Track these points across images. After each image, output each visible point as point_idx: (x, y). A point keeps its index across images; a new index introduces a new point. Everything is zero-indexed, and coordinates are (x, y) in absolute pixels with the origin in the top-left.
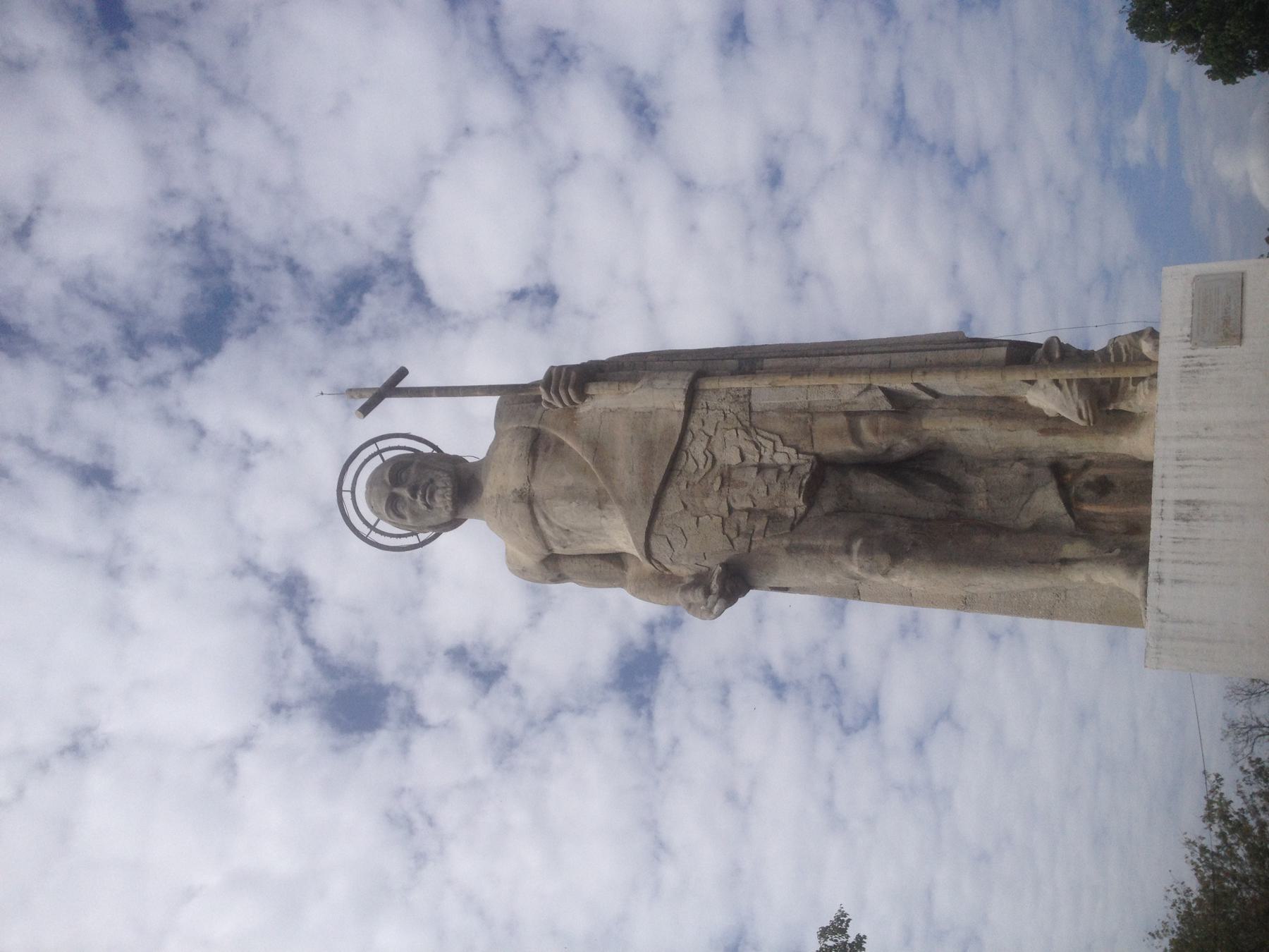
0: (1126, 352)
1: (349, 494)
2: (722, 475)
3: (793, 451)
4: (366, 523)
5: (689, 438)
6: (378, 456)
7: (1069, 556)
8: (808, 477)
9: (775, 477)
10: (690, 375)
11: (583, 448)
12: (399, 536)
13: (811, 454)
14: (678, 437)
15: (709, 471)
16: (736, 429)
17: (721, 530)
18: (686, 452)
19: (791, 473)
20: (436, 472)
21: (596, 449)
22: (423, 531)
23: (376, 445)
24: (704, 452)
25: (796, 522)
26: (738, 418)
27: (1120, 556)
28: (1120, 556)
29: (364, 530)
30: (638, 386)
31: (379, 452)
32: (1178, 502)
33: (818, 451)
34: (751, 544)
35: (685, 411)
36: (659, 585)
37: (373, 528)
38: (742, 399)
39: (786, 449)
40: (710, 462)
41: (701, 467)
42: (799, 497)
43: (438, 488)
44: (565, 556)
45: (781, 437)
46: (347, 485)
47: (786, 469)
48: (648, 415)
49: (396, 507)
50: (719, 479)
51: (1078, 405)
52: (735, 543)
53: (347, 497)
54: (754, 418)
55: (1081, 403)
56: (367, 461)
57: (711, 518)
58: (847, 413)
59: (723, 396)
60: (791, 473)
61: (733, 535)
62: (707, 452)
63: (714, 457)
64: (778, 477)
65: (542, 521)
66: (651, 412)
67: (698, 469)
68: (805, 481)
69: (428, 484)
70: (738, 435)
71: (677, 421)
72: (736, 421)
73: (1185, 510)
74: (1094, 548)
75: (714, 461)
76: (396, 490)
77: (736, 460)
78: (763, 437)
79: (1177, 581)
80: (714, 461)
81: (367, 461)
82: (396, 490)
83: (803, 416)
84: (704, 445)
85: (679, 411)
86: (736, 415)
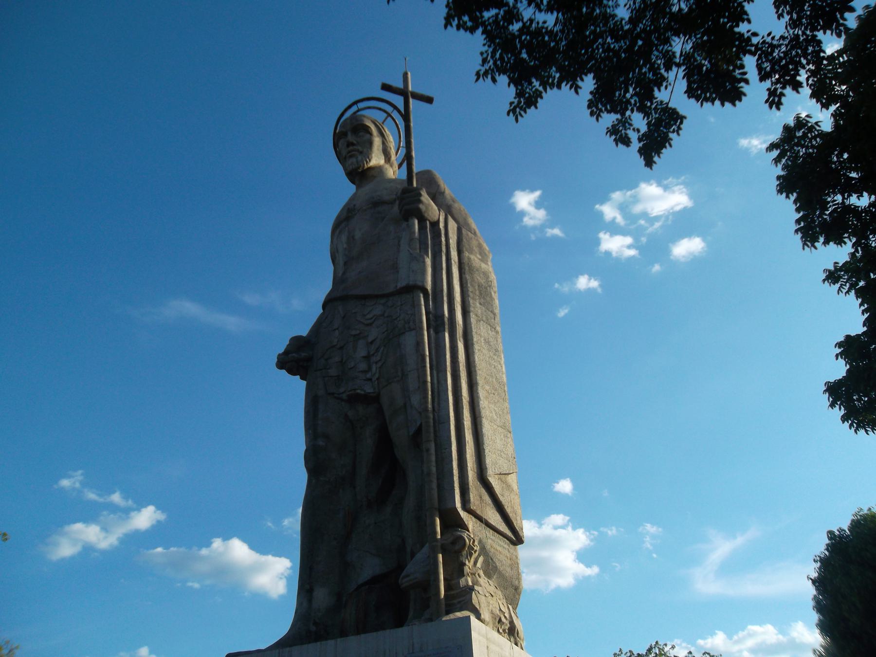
2: (360, 333)
3: (377, 375)
5: (383, 301)
6: (385, 115)
8: (363, 392)
16: (387, 331)
19: (365, 380)
25: (336, 395)
31: (389, 115)
34: (321, 370)
38: (407, 326)
40: (369, 322)
41: (368, 316)
42: (350, 391)
45: (384, 363)
47: (369, 376)
50: (358, 332)
56: (380, 109)
59: (409, 312)
60: (365, 380)
63: (373, 323)
64: (362, 372)
65: (338, 231)
68: (359, 391)
69: (358, 151)
71: (391, 289)
75: (371, 324)
76: (349, 134)
78: (383, 350)
80: (371, 324)
81: (380, 109)
83: (400, 374)
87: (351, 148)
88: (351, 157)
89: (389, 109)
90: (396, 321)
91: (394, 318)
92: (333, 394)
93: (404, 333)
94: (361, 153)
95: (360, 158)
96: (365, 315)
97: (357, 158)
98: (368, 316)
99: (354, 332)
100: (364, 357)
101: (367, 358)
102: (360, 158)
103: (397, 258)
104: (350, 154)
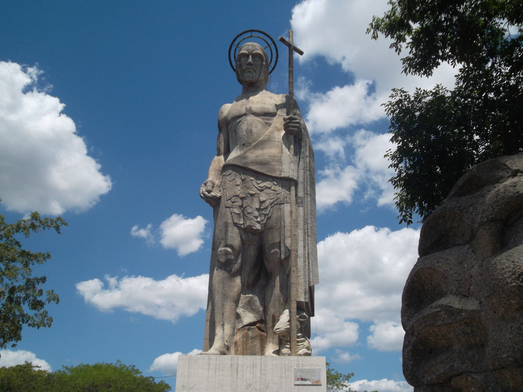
0: (302, 345)
1: (249, 36)
4: (239, 44)
6: (267, 45)
7: (225, 327)
9: (255, 215)
10: (295, 178)
11: (267, 135)
12: (235, 58)
13: (264, 229)
14: (271, 175)
15: (257, 189)
16: (273, 199)
17: (234, 195)
18: (265, 179)
20: (259, 72)
21: (266, 141)
22: (236, 67)
23: (267, 47)
24: (265, 186)
26: (278, 199)
27: (225, 345)
28: (225, 345)
29: (236, 43)
30: (292, 157)
32: (238, 364)
33: (265, 232)
35: (281, 177)
36: (216, 170)
37: (237, 46)
38: (285, 200)
39: (265, 219)
41: (259, 185)
43: (252, 74)
44: (228, 129)
46: (254, 34)
48: (280, 161)
49: (244, 57)
50: (254, 193)
51: (281, 328)
52: (230, 201)
53: (249, 34)
54: (278, 206)
55: (282, 329)
56: (265, 41)
57: (239, 191)
58: (280, 242)
61: (232, 200)
62: (265, 187)
66: (281, 163)
67: (258, 184)
69: (254, 70)
70: (271, 199)
71: (277, 174)
72: (277, 198)
73: (235, 366)
74: (228, 335)
75: (261, 191)
76: (250, 56)
77: (262, 199)
78: (270, 209)
79: (209, 364)
81: (265, 41)
82: (250, 56)
84: (268, 186)
85: (281, 174)
86: (279, 198)
87: (250, 67)
88: (249, 72)
89: (270, 42)
90: (279, 195)
91: (278, 193)
92: (236, 224)
93: (283, 204)
94: (255, 71)
95: (254, 74)
96: (258, 184)
97: (252, 74)
98: (259, 185)
99: (251, 192)
100: (256, 209)
101: (258, 210)
102: (254, 74)
103: (281, 156)
104: (248, 70)
